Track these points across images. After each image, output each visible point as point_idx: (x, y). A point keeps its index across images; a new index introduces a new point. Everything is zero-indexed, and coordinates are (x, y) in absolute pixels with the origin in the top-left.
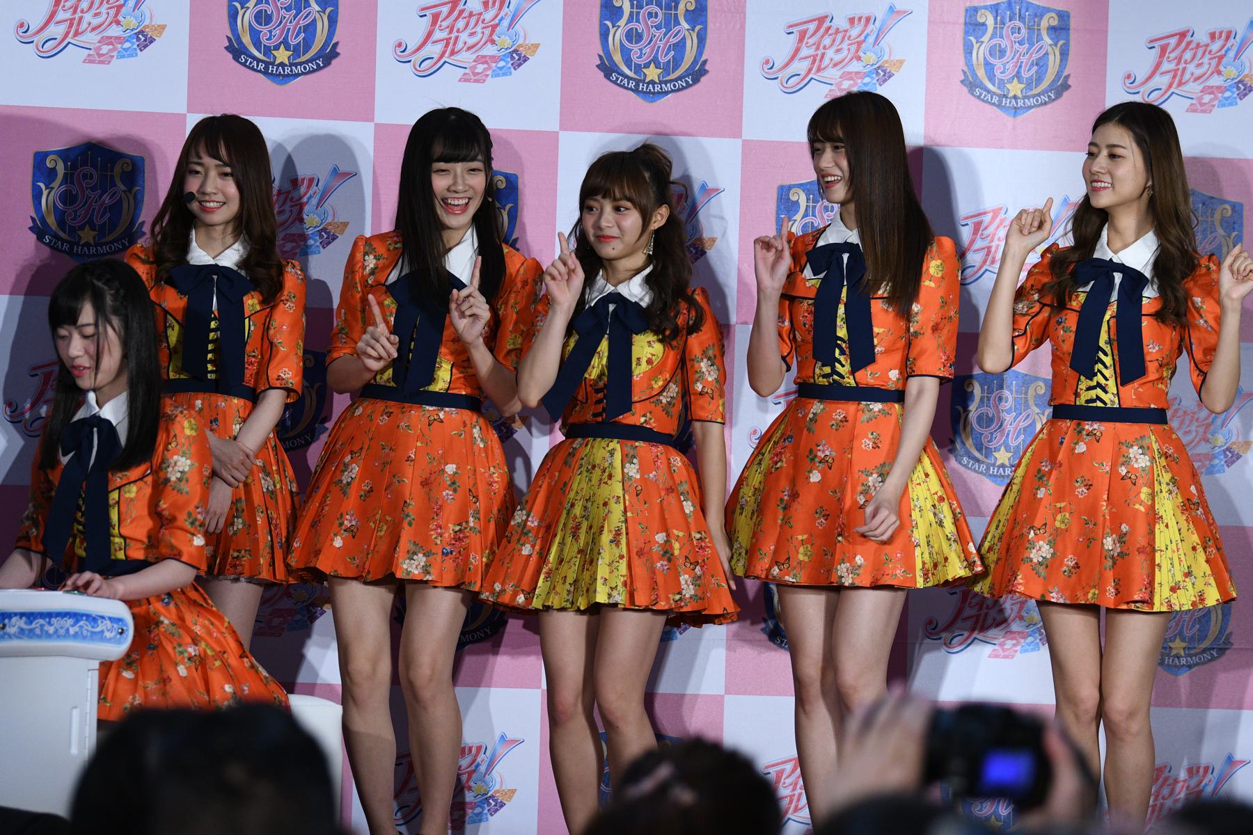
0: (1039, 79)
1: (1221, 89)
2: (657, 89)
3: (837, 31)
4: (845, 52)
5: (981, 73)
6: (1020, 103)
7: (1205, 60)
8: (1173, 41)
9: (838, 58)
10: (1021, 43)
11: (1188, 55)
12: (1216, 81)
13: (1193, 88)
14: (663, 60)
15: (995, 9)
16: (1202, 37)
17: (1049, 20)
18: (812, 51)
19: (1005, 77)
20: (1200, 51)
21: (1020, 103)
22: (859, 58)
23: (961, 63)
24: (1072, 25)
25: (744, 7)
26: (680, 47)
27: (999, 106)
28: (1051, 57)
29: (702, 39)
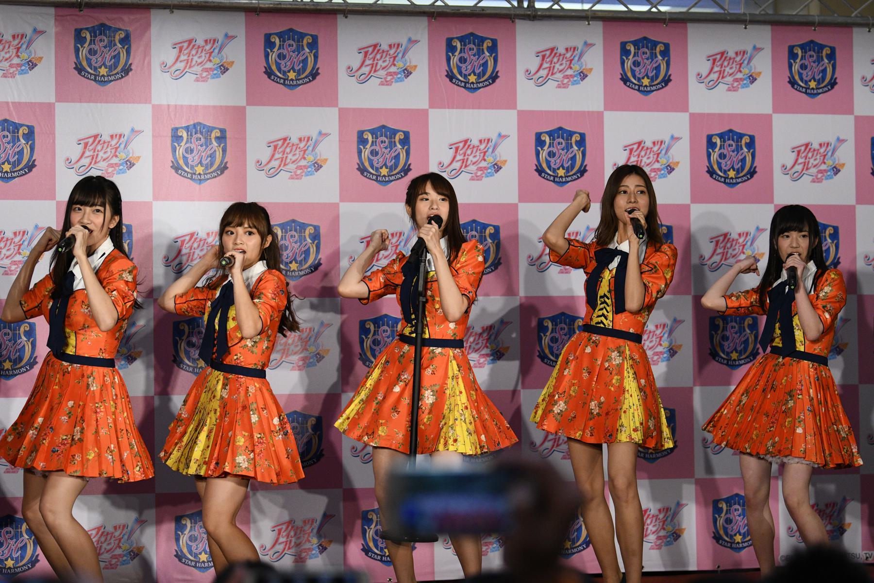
0: (212, 164)
1: (306, 167)
2: (9, 175)
3: (104, 142)
4: (109, 153)
5: (181, 162)
6: (202, 177)
7: (297, 152)
8: (280, 143)
9: (105, 156)
10: (202, 146)
11: (288, 150)
12: (303, 163)
13: (292, 167)
14: (12, 160)
15: (187, 128)
16: (295, 140)
17: (216, 133)
18: (91, 153)
19: (194, 164)
20: (294, 148)
21: (202, 177)
22: (116, 156)
23: (170, 157)
24: (228, 135)
25: (54, 131)
26: (21, 153)
27: (191, 179)
28: (217, 153)
29: (32, 149)
